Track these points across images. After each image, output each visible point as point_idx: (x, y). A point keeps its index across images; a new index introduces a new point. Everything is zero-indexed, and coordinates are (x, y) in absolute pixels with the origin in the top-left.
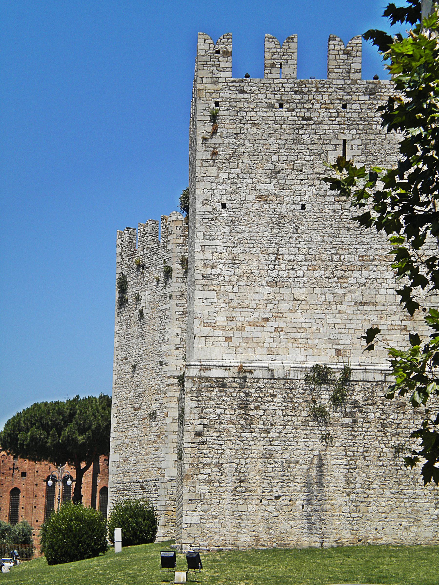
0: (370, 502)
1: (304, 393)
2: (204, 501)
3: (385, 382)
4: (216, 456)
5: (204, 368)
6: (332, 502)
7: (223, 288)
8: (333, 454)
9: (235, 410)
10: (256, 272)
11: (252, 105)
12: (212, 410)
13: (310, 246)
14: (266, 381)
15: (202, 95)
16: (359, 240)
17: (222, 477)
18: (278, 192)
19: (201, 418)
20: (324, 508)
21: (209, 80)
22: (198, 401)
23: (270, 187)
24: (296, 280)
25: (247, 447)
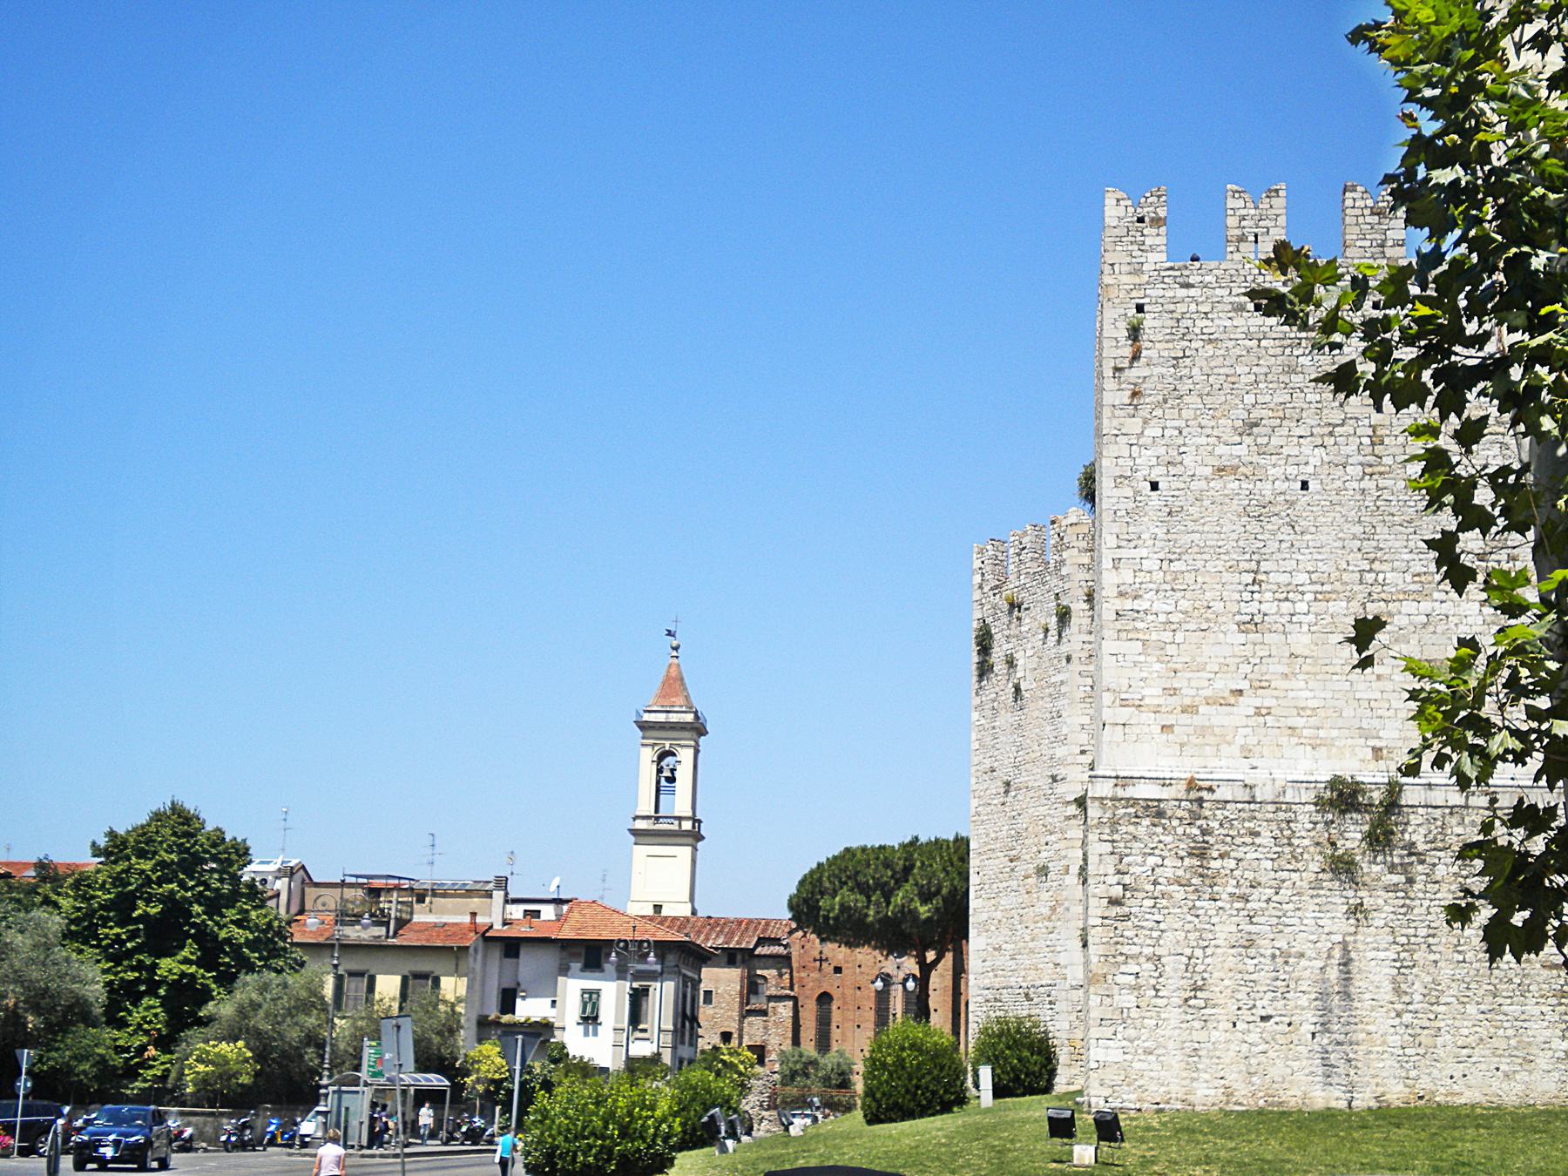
0: (1439, 1029)
1: (1314, 829)
2: (1129, 1021)
3: (1466, 807)
4: (1149, 942)
5: (1122, 781)
6: (1368, 1027)
7: (1154, 636)
8: (1369, 940)
9: (1182, 858)
10: (1218, 606)
11: (1205, 308)
12: (1139, 859)
13: (1319, 557)
14: (1240, 806)
15: (1113, 293)
16: (1411, 544)
17: (1160, 980)
18: (1255, 459)
19: (1119, 872)
20: (1354, 1039)
21: (1125, 268)
22: (1113, 841)
23: (1241, 450)
24: (1295, 619)
25: (1207, 927)
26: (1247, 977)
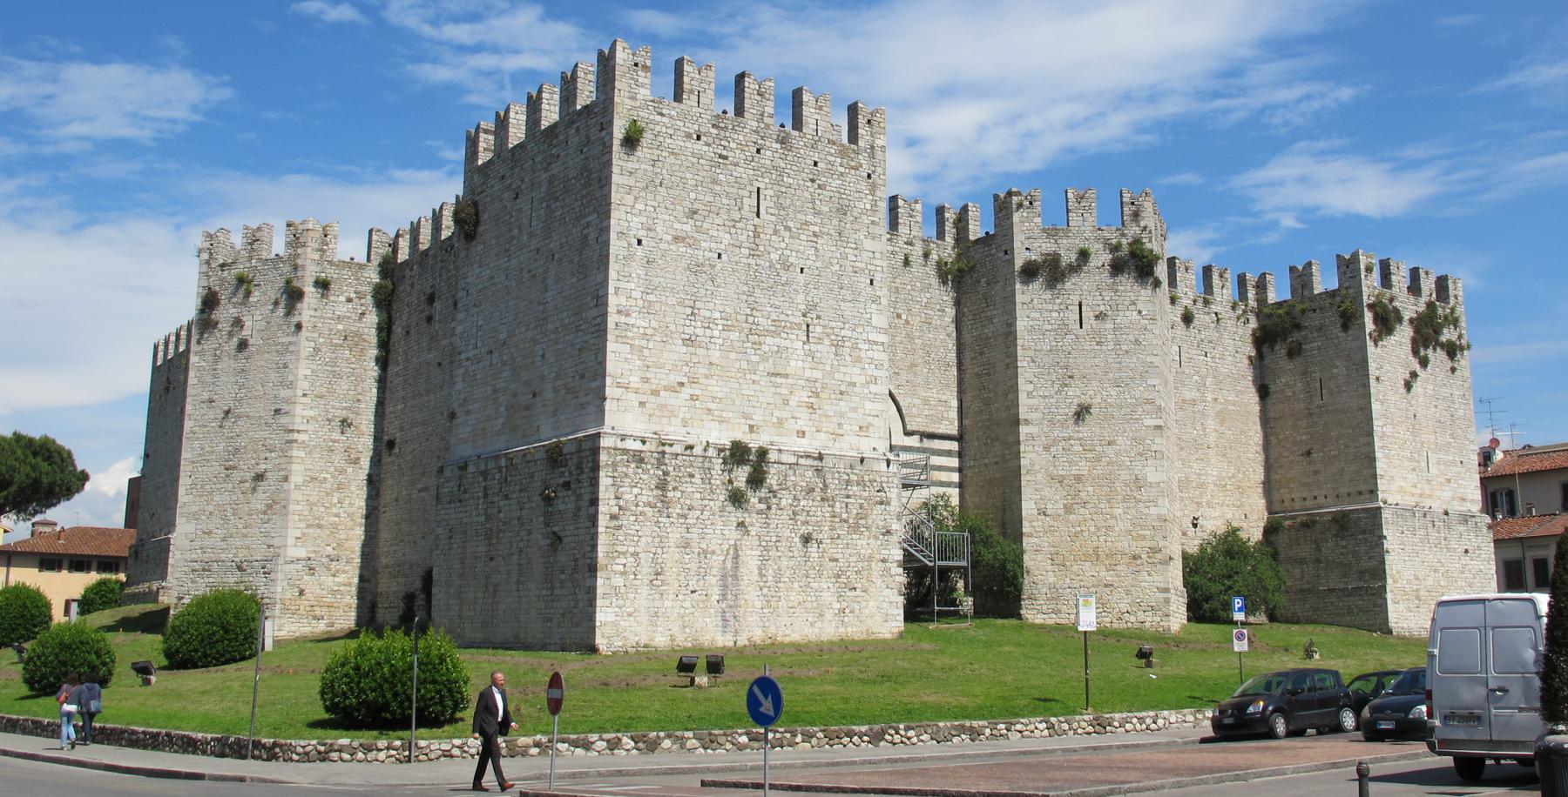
3: (797, 464)
7: (637, 342)
10: (672, 327)
18: (696, 235)
19: (617, 498)
21: (627, 94)
22: (614, 477)
23: (687, 228)
24: (712, 340)
26: (685, 566)
